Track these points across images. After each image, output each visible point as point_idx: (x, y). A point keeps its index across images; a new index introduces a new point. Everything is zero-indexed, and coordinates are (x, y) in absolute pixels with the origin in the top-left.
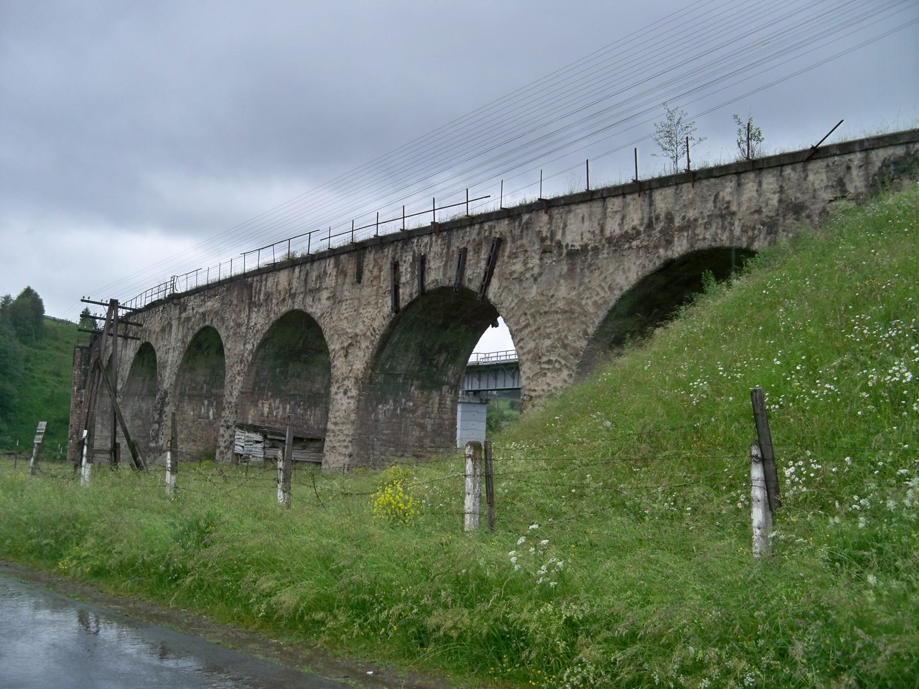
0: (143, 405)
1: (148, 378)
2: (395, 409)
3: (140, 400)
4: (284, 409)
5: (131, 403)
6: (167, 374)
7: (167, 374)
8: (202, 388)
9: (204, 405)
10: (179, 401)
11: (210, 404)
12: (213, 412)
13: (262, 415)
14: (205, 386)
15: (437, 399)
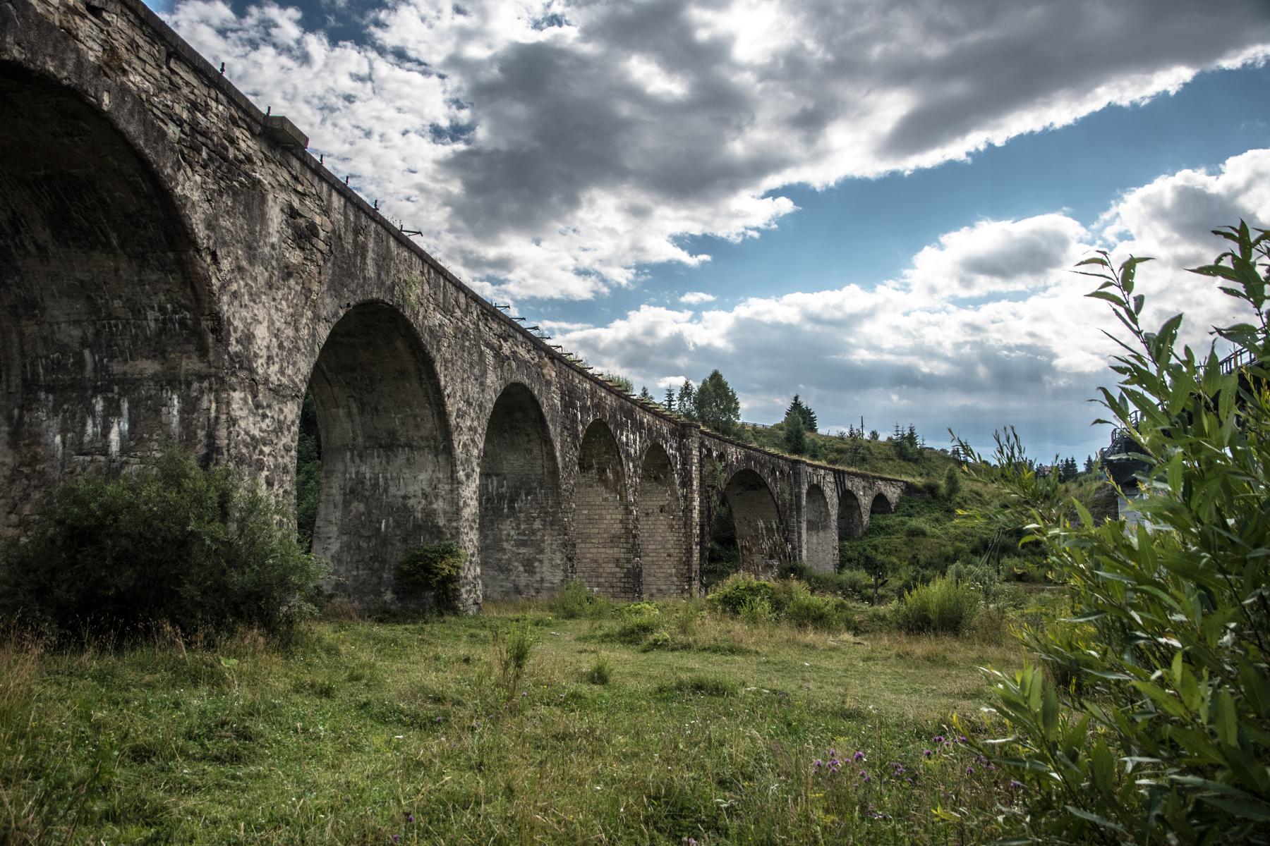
0: (363, 468)
1: (355, 411)
3: (357, 460)
5: (340, 467)
8: (80, 363)
9: (92, 412)
10: (22, 408)
11: (112, 410)
12: (121, 434)
14: (87, 353)
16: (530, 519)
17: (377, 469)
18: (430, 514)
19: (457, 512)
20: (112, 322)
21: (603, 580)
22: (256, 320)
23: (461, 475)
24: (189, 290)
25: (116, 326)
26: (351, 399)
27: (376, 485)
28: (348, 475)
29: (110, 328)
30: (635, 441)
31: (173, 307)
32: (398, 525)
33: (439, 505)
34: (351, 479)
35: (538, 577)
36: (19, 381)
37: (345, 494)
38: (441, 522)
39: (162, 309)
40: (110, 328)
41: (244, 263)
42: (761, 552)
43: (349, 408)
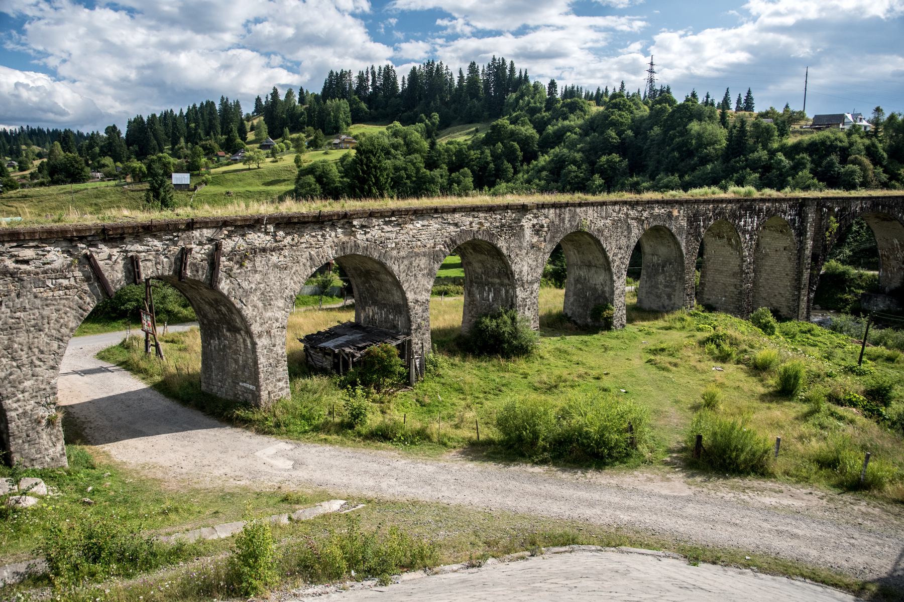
0: (581, 272)
1: (576, 253)
2: (220, 345)
4: (381, 314)
5: (573, 271)
8: (482, 277)
9: (485, 290)
11: (490, 290)
13: (369, 317)
15: (241, 340)
16: (671, 276)
18: (604, 292)
19: (613, 293)
21: (727, 294)
22: (523, 266)
23: (615, 278)
27: (585, 279)
30: (752, 222)
32: (593, 295)
33: (607, 289)
35: (673, 302)
38: (607, 295)
41: (518, 252)
42: (896, 259)
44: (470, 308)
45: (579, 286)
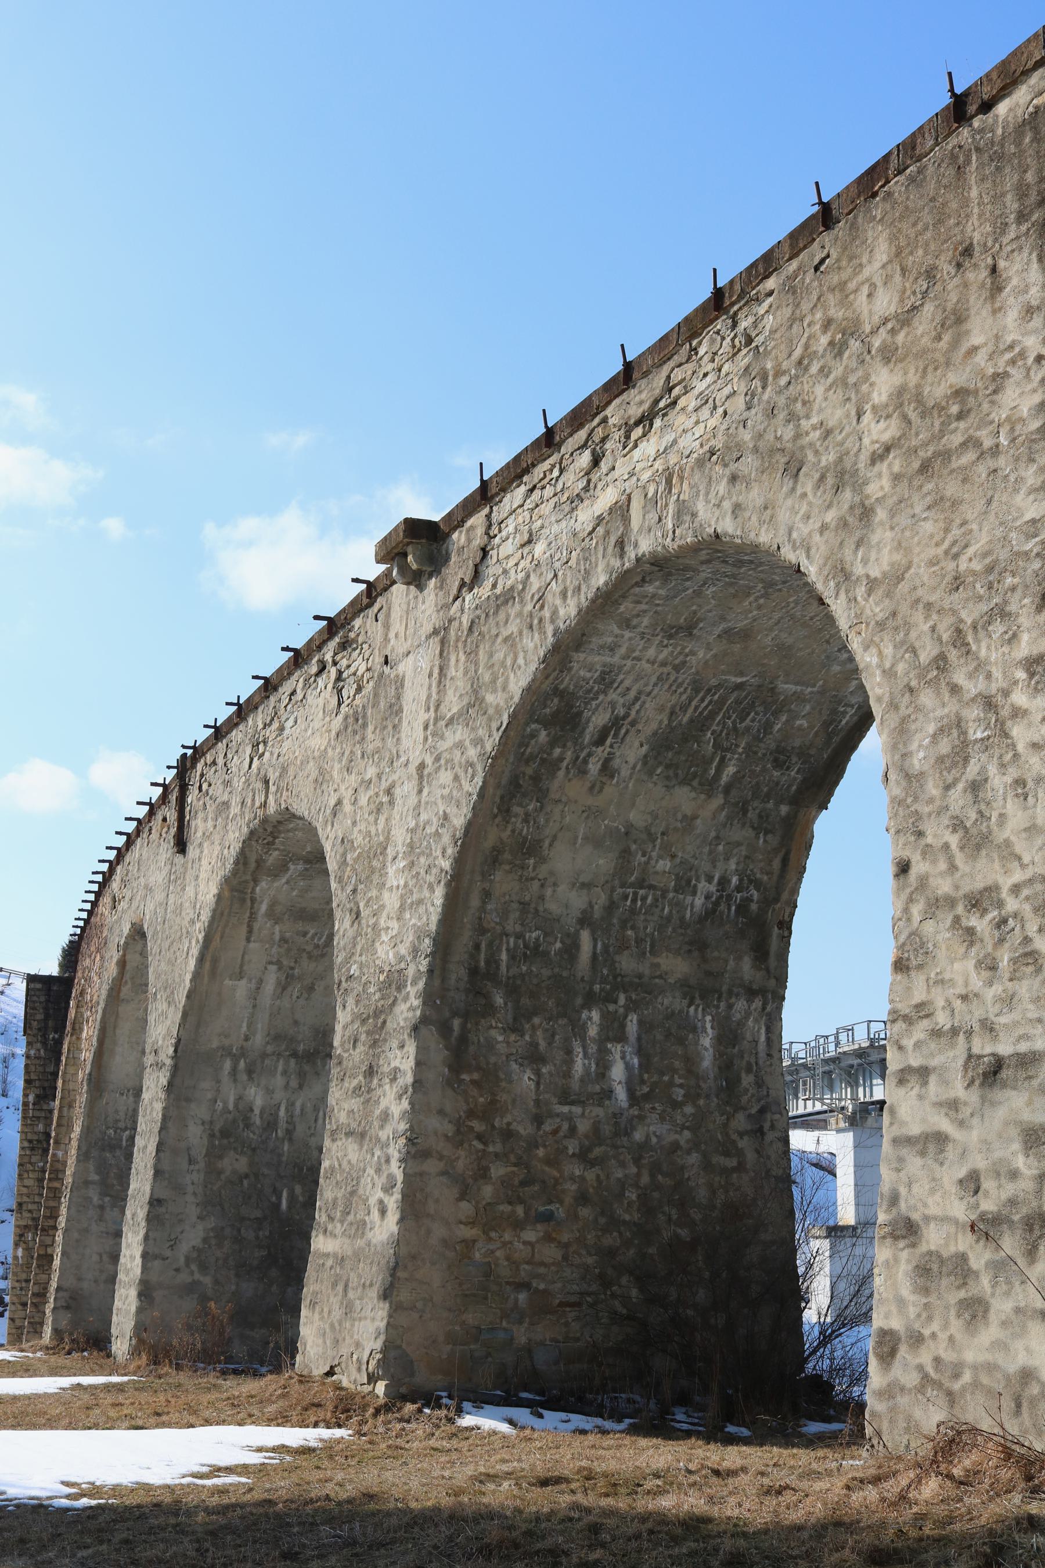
3: (244, 1077)
6: (391, 900)
7: (391, 900)
8: (571, 949)
9: (579, 1029)
10: (466, 1016)
14: (585, 936)
17: (279, 1095)
20: (642, 892)
24: (777, 864)
25: (644, 899)
26: (273, 968)
27: (271, 1124)
28: (220, 1105)
29: (634, 901)
31: (741, 880)
34: (226, 1110)
36: (463, 973)
37: (212, 1136)
39: (723, 882)
40: (634, 901)
43: (261, 981)
44: (463, 1162)
45: (235, 1163)
